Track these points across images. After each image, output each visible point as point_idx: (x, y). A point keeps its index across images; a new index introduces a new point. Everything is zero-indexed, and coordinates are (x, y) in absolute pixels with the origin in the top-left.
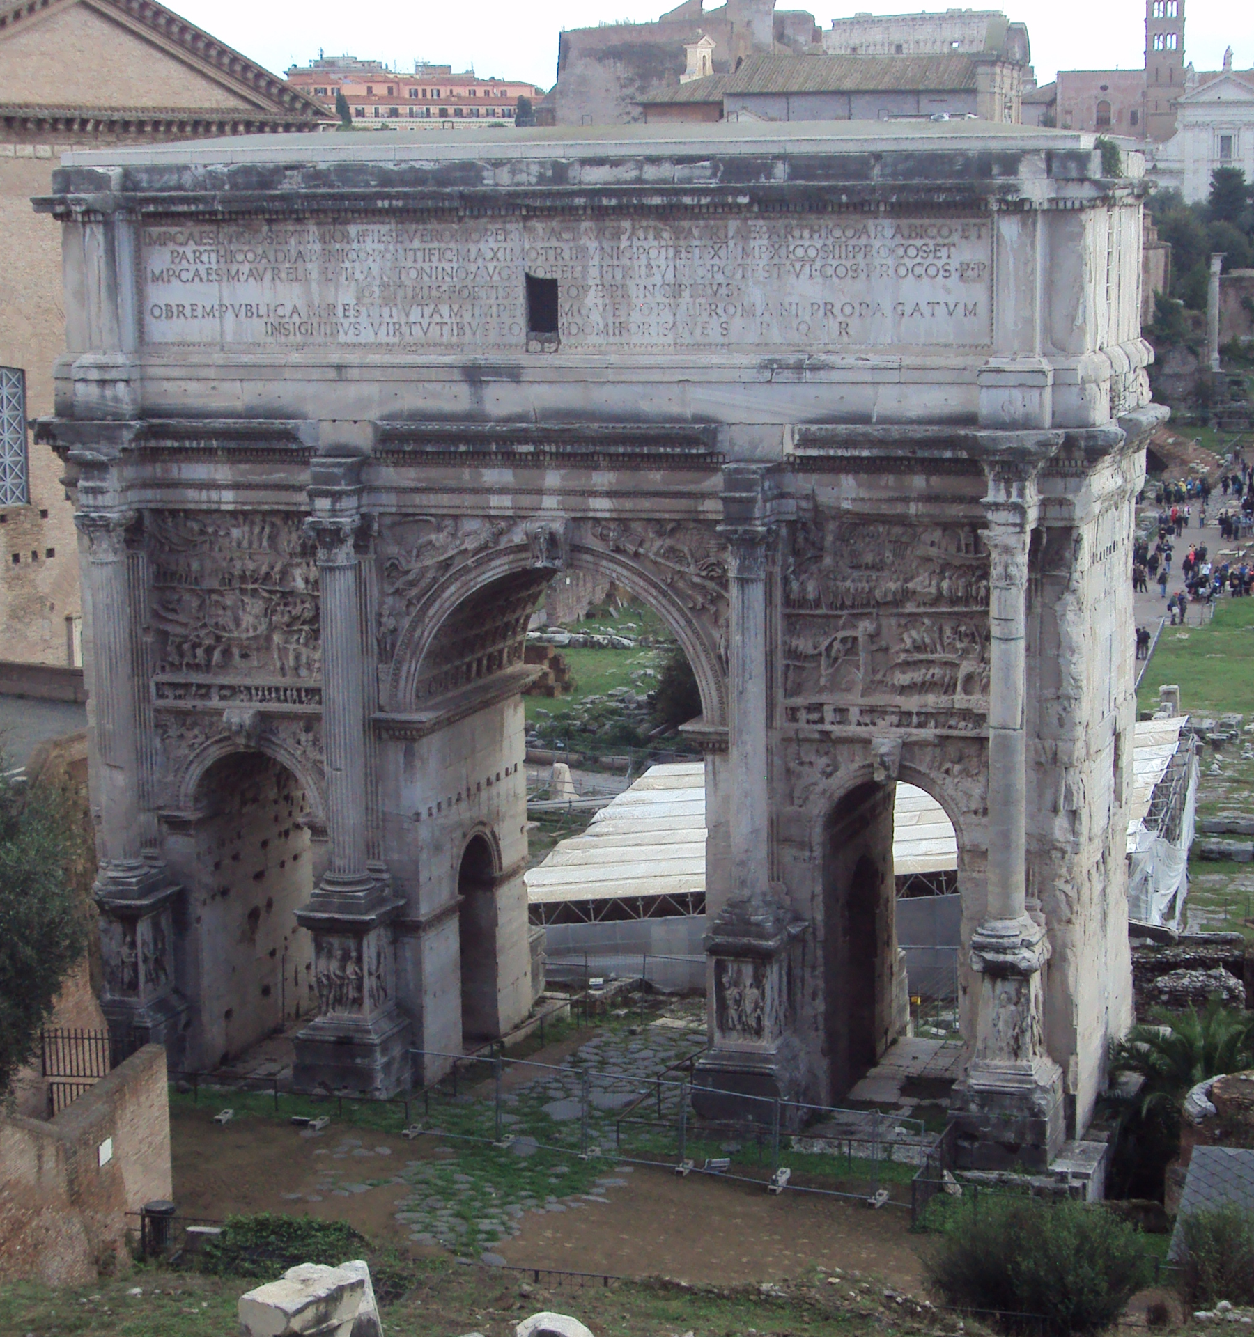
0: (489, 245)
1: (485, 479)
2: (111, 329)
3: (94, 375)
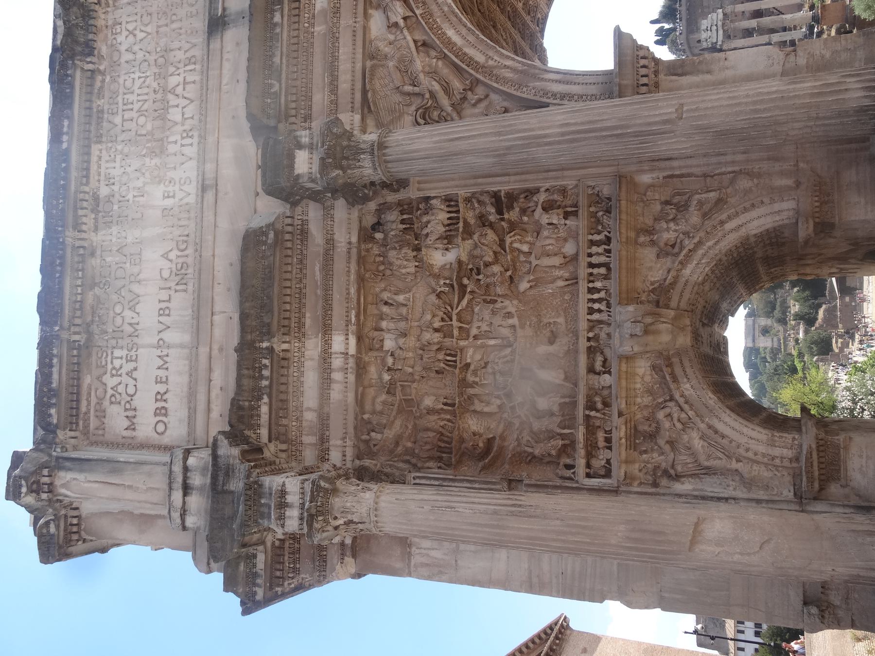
0: (124, 40)
1: (325, 5)
2: (150, 474)
3: (177, 496)
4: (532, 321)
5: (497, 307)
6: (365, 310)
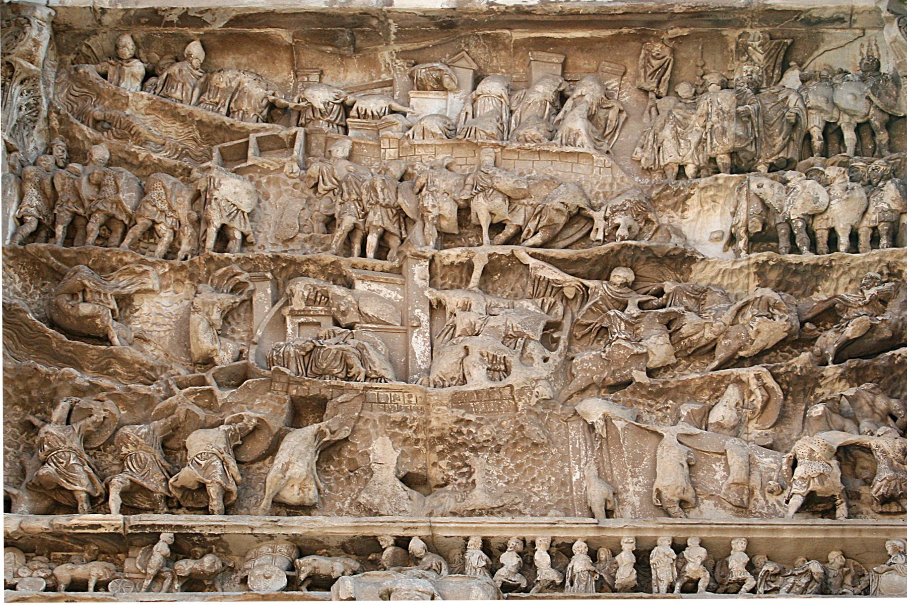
4: (479, 426)
5: (531, 345)
6: (543, 44)
